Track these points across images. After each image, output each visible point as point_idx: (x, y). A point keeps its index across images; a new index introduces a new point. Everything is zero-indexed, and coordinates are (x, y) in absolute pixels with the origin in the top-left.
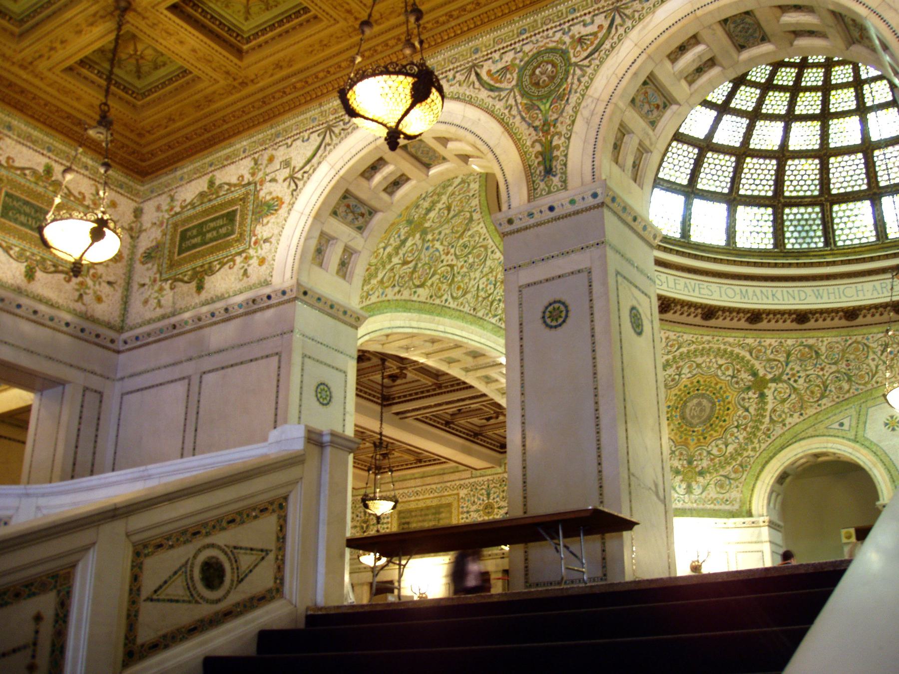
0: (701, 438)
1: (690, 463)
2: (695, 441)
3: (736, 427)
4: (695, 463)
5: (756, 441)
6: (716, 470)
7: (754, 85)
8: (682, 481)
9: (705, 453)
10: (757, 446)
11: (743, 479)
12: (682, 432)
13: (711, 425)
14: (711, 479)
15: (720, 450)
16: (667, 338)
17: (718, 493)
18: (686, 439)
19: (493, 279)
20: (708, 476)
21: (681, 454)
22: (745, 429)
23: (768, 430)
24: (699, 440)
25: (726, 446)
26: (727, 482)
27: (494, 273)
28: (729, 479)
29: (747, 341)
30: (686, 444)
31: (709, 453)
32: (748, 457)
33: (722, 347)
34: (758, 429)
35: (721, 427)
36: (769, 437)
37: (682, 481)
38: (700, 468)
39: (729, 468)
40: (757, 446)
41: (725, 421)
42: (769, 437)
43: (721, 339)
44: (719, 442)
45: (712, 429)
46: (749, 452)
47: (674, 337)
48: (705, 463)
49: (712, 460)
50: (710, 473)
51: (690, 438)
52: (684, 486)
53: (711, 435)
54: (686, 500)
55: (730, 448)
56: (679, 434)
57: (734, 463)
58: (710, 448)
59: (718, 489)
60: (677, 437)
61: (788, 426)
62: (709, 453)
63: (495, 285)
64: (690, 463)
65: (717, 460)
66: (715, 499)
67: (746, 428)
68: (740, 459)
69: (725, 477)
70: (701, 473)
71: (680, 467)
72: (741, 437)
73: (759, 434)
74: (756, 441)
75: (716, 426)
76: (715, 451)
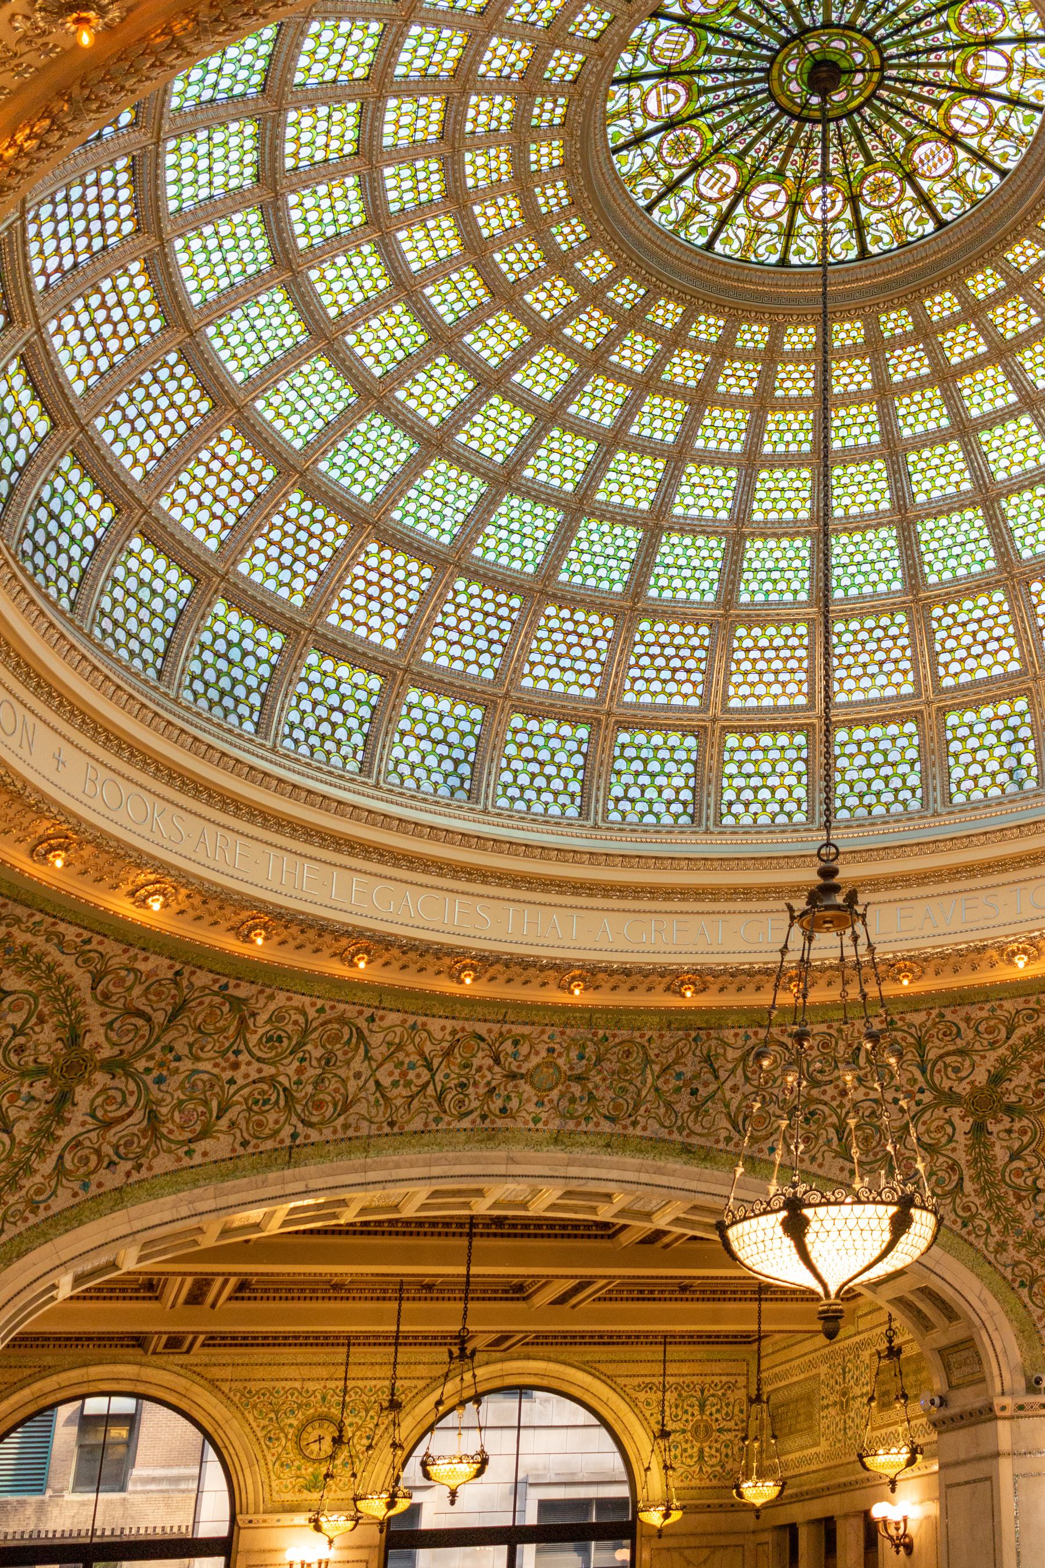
19: (414, 1058)
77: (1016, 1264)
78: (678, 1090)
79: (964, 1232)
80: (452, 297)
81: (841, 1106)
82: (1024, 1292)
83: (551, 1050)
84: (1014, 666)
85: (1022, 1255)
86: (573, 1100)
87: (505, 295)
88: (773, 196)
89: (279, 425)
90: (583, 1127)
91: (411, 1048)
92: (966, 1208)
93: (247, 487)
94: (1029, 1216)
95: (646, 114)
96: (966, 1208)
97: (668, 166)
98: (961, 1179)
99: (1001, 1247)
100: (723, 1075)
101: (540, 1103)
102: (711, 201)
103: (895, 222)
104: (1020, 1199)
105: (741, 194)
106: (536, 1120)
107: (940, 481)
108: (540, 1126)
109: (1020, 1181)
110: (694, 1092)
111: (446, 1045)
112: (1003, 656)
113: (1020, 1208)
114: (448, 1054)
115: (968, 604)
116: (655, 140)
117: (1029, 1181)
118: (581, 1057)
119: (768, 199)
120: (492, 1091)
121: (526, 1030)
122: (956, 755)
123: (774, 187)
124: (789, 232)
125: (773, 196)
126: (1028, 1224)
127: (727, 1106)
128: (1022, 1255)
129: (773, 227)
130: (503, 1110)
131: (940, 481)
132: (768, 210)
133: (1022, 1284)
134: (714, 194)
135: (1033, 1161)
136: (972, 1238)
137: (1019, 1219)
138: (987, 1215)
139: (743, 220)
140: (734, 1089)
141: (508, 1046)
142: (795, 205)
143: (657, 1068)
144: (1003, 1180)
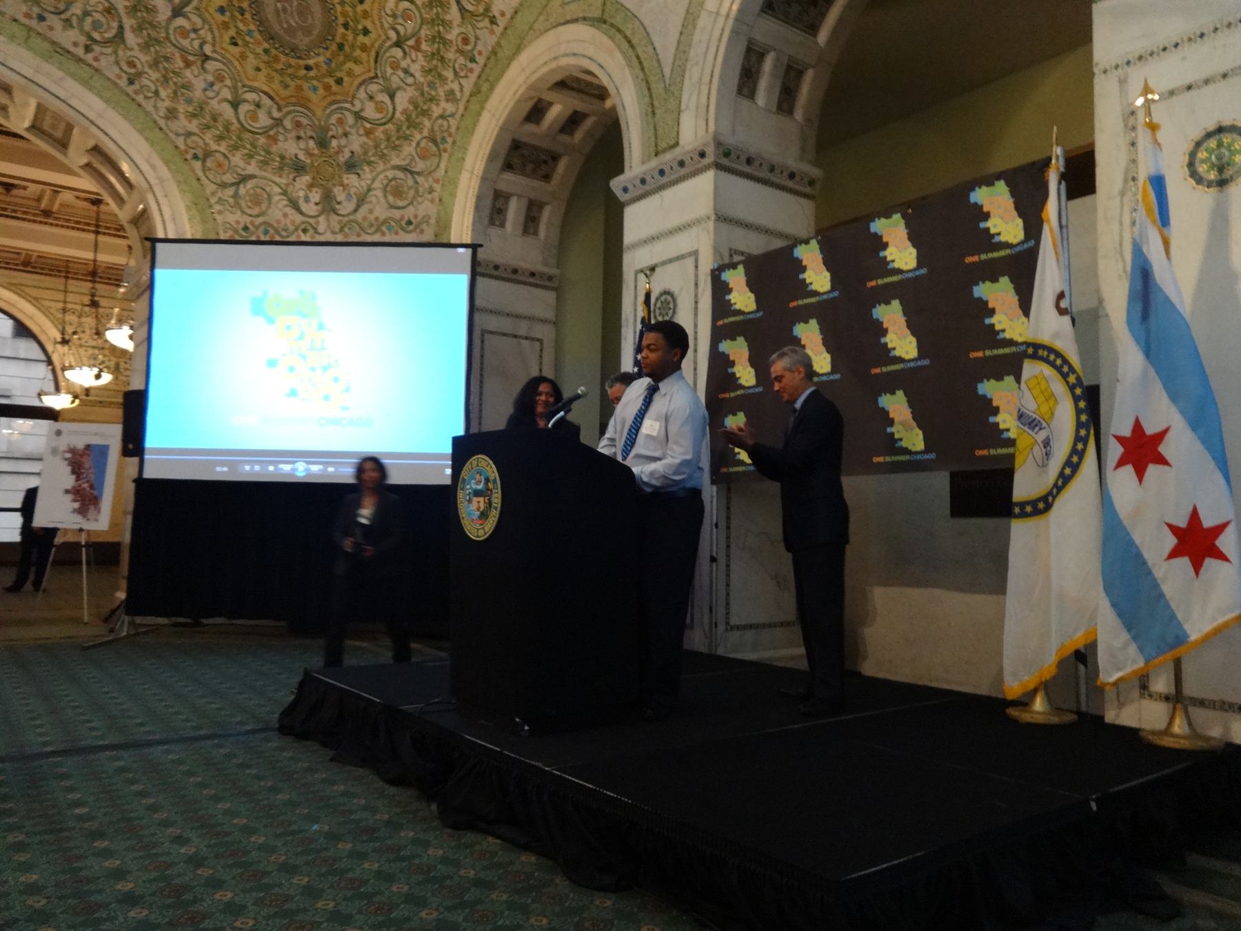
0: (331, 81)
1: (323, 143)
2: (321, 91)
3: (398, 44)
4: (334, 143)
5: (449, 74)
6: (383, 156)
8: (311, 186)
9: (350, 119)
10: (456, 87)
11: (440, 173)
12: (281, 72)
13: (341, 47)
14: (372, 178)
15: (380, 107)
17: (392, 207)
18: (299, 89)
20: (367, 173)
21: (298, 125)
22: (417, 48)
23: (466, 41)
24: (327, 87)
25: (392, 97)
26: (410, 182)
28: (412, 173)
30: (303, 102)
31: (358, 116)
32: (442, 117)
34: (445, 42)
35: (364, 48)
36: (473, 60)
37: (311, 186)
38: (347, 155)
39: (409, 149)
40: (456, 87)
41: (366, 32)
42: (473, 60)
44: (373, 88)
45: (348, 58)
46: (443, 104)
48: (356, 143)
49: (368, 133)
50: (369, 163)
51: (305, 85)
52: (316, 196)
53: (350, 73)
54: (321, 229)
55: (402, 100)
56: (277, 78)
57: (418, 137)
58: (357, 109)
59: (391, 199)
60: (276, 85)
61: (502, 22)
62: (358, 116)
64: (323, 143)
65: (379, 133)
66: (385, 221)
67: (418, 42)
68: (427, 123)
69: (404, 169)
70: (351, 166)
71: (302, 156)
72: (415, 69)
73: (450, 55)
74: (449, 74)
75: (353, 47)
76: (370, 112)
77: (189, 134)
79: (130, 89)
82: (197, 165)
85: (193, 126)
92: (131, 64)
94: (199, 84)
96: (131, 64)
98: (121, 27)
99: (172, 114)
104: (188, 64)
109: (185, 43)
113: (188, 73)
117: (196, 43)
126: (198, 94)
128: (193, 126)
133: (195, 157)
135: (198, 21)
136: (140, 98)
137: (187, 86)
138: (155, 75)
144: (168, 38)
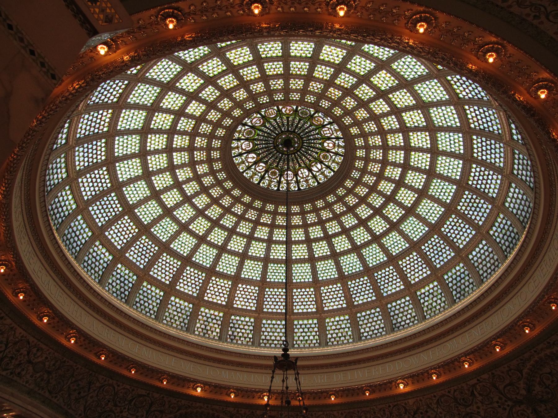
7: (242, 235)
16: (169, 401)
27: (6, 335)
29: (228, 409)
33: (211, 412)
43: (209, 406)
47: (175, 402)
63: (6, 345)
78: (75, 390)
80: (184, 124)
81: (118, 416)
83: (46, 358)
84: (224, 303)
86: (42, 380)
87: (194, 134)
88: (254, 158)
89: (121, 119)
90: (40, 392)
91: (6, 335)
93: (98, 128)
95: (251, 122)
97: (243, 135)
100: (91, 390)
101: (32, 376)
102: (242, 149)
103: (270, 183)
105: (248, 152)
106: (27, 382)
107: (236, 246)
108: (27, 385)
110: (79, 393)
111: (17, 340)
112: (223, 299)
114: (15, 344)
115: (222, 281)
116: (247, 127)
118: (54, 365)
119: (252, 158)
120: (19, 365)
121: (44, 347)
122: (199, 320)
123: (255, 156)
124: (249, 168)
125: (254, 158)
127: (86, 402)
129: (247, 164)
130: (19, 373)
131: (236, 246)
132: (250, 160)
134: (244, 148)
139: (243, 158)
140: (92, 397)
141: (35, 350)
142: (255, 163)
143: (74, 379)
